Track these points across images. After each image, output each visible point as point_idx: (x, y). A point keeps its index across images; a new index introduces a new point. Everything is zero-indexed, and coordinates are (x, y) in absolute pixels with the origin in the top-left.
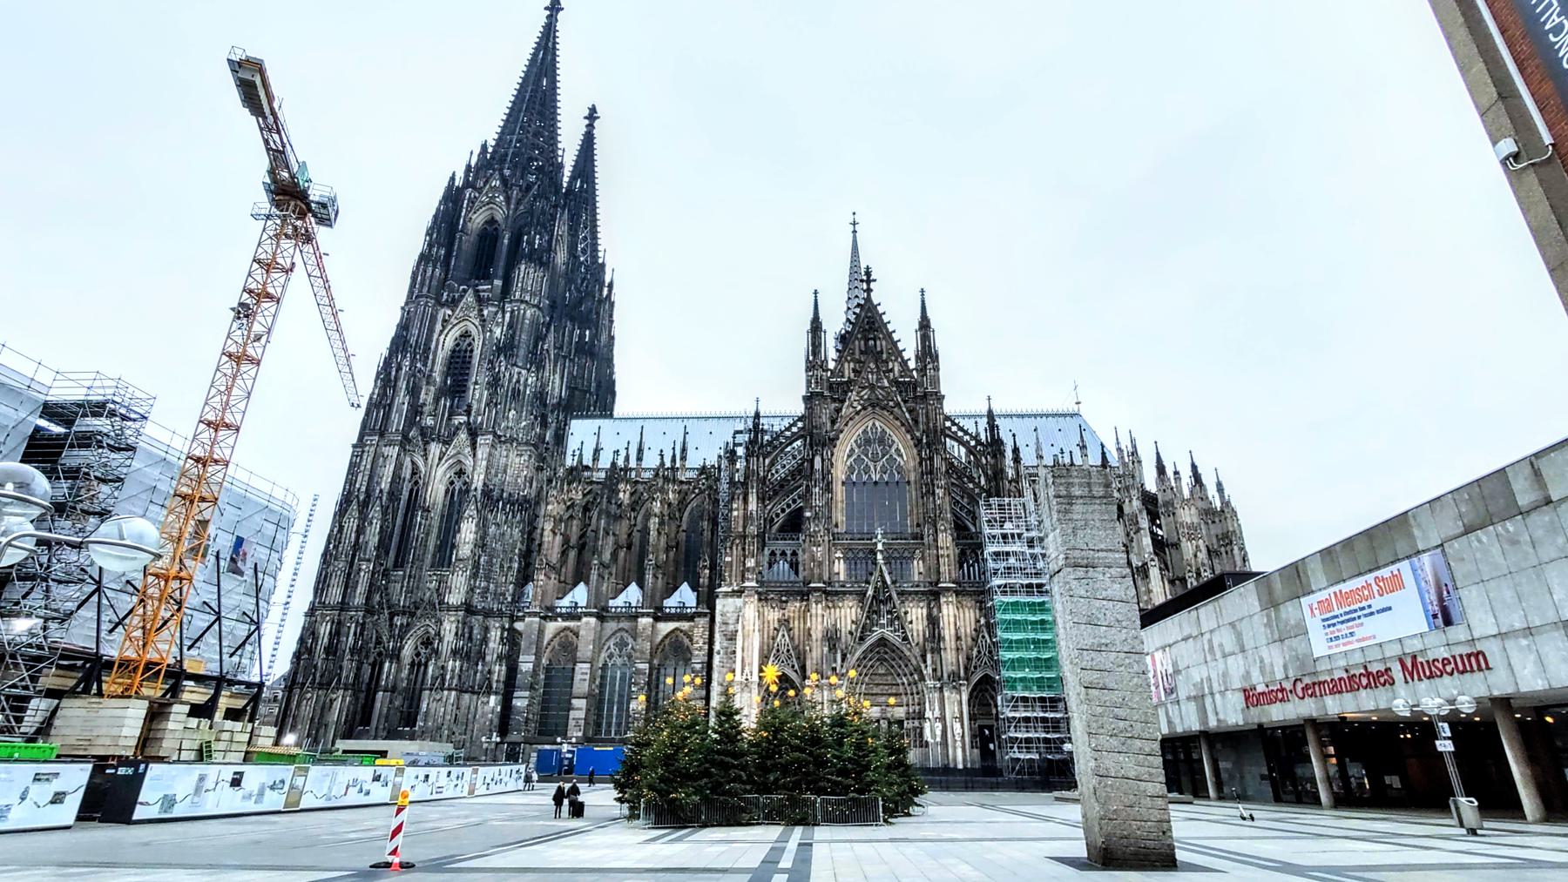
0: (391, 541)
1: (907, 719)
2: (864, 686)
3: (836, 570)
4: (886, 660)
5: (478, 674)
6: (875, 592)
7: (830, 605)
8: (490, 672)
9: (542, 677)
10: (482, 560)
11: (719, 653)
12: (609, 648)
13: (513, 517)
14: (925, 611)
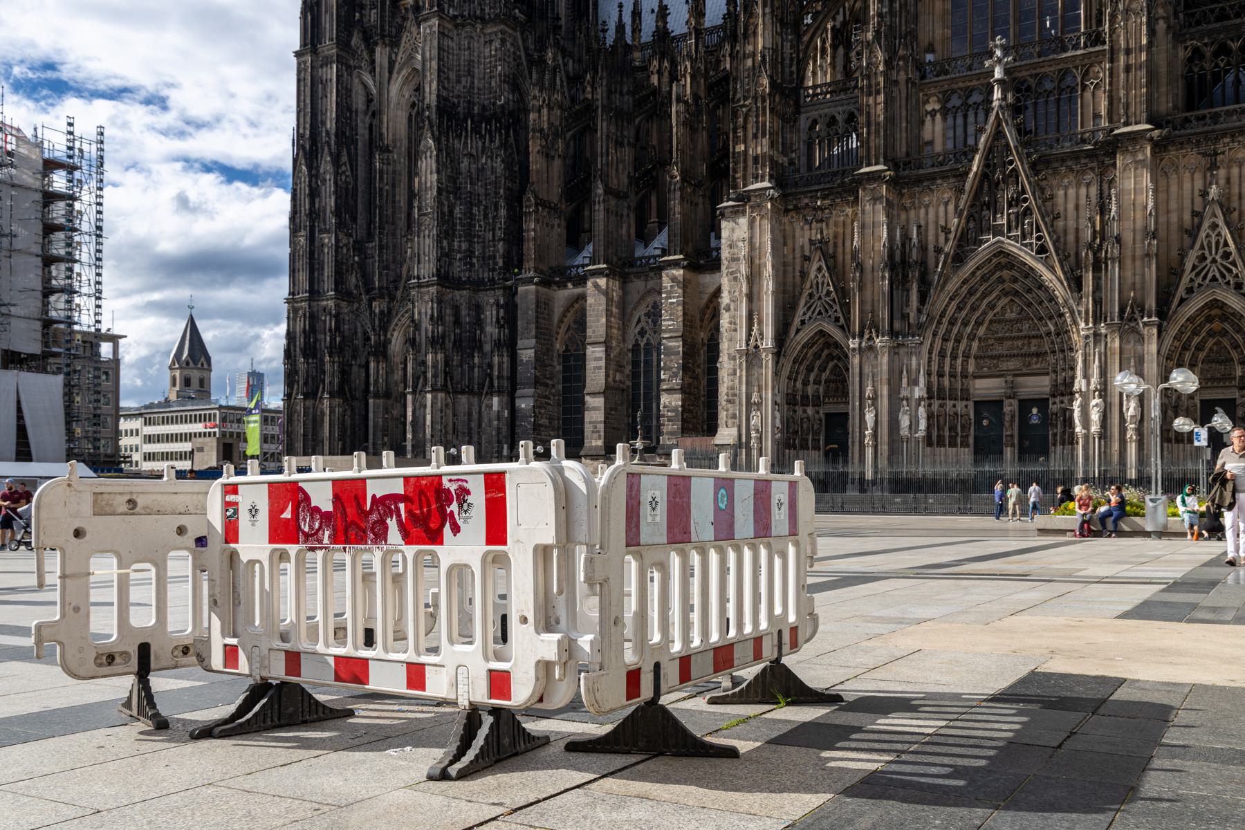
0: (356, 201)
1: (1054, 396)
2: (975, 345)
3: (927, 135)
4: (1017, 293)
5: (476, 370)
6: (987, 166)
7: (908, 202)
8: (490, 366)
9: (559, 368)
10: (457, 210)
11: (728, 309)
12: (639, 321)
13: (491, 141)
14: (1094, 190)
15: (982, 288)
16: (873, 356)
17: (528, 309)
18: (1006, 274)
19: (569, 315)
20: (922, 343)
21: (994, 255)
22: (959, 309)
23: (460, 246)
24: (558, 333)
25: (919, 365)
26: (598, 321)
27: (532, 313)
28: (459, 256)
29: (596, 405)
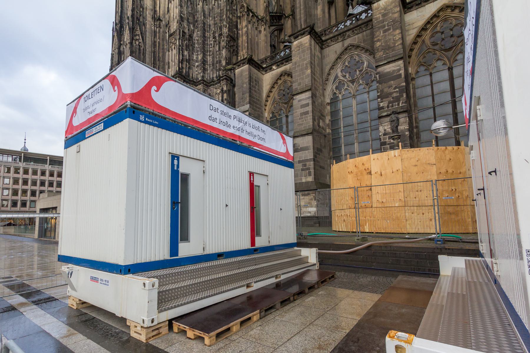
17: (243, 84)
19: (274, 90)
23: (197, 58)
24: (266, 106)
26: (304, 73)
27: (246, 86)
28: (197, 64)
29: (305, 145)
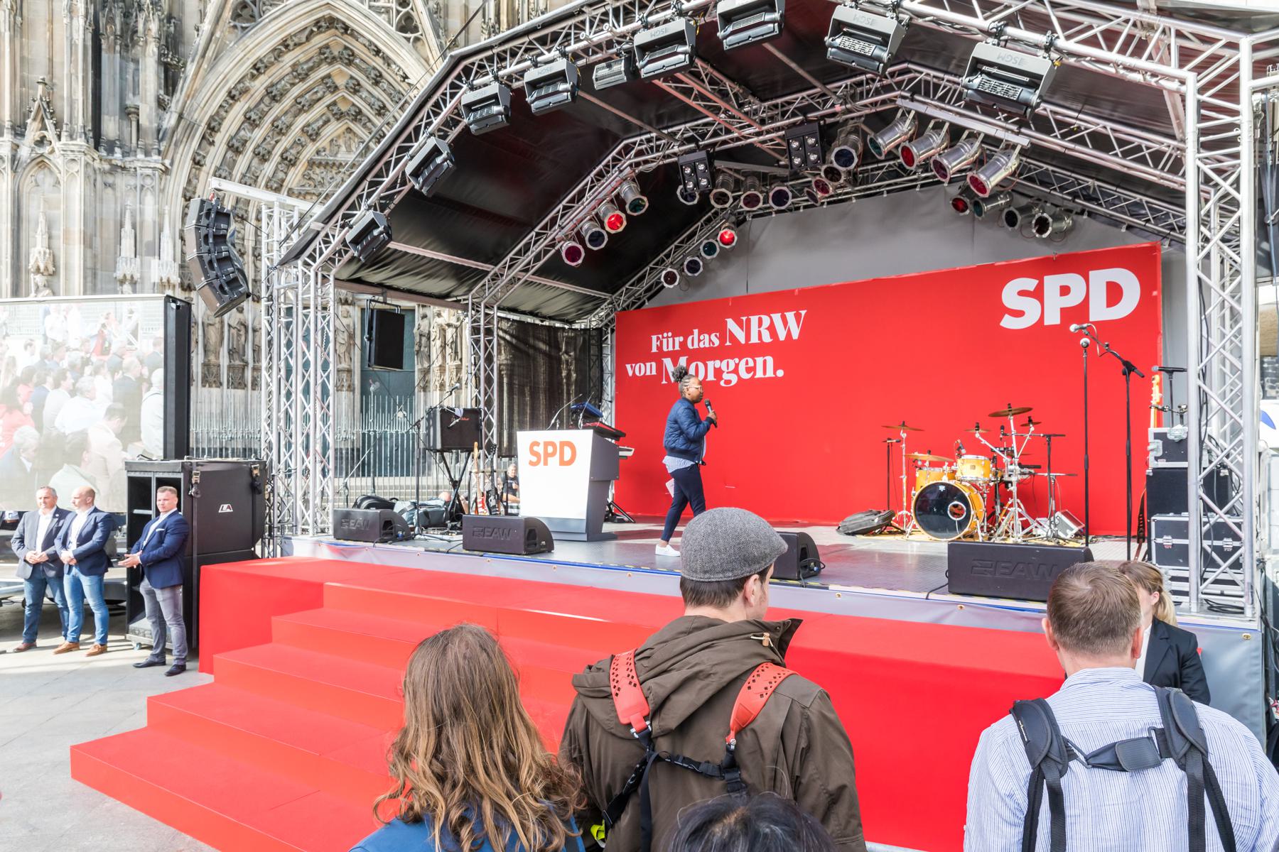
4: (358, 115)
15: (296, 91)
16: (49, 181)
18: (341, 74)
20: (166, 171)
21: (317, 23)
22: (251, 121)
25: (161, 214)
